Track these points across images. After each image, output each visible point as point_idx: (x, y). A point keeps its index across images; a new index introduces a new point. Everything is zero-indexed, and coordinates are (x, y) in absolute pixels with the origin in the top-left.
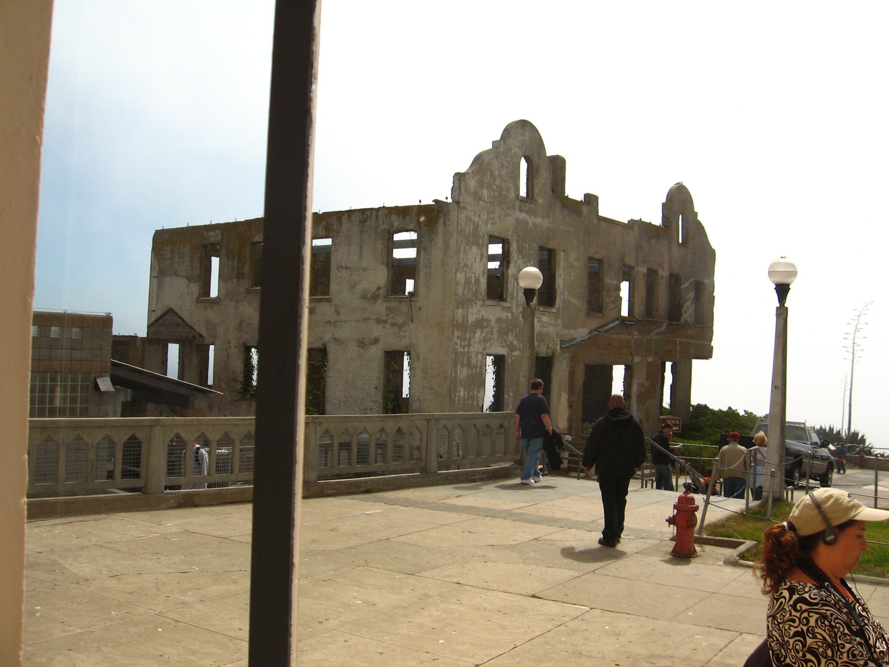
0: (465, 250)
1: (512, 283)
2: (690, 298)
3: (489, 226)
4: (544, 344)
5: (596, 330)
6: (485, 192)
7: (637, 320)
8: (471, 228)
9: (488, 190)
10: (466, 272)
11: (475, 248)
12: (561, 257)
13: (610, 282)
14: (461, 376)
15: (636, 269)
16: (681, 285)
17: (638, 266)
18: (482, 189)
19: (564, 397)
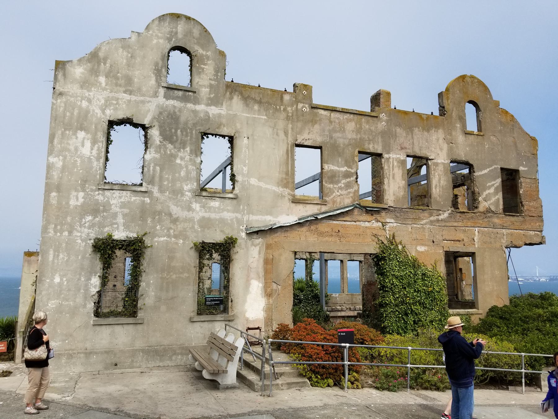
0: (63, 134)
1: (151, 168)
2: (493, 185)
3: (108, 112)
4: (216, 230)
5: (310, 216)
6: (102, 79)
7: (389, 207)
8: (75, 113)
9: (106, 77)
10: (65, 157)
11: (81, 134)
12: (242, 143)
13: (335, 168)
14: (56, 261)
15: (386, 156)
16: (474, 172)
17: (388, 153)
18: (97, 76)
19: (256, 286)
